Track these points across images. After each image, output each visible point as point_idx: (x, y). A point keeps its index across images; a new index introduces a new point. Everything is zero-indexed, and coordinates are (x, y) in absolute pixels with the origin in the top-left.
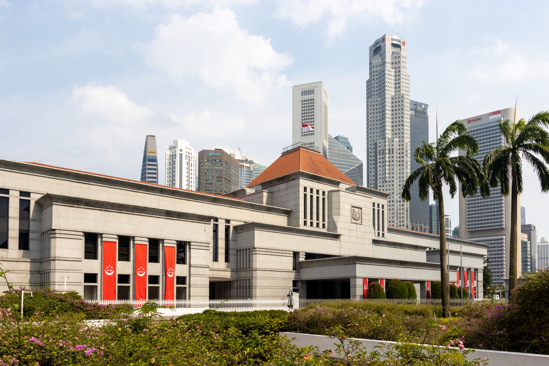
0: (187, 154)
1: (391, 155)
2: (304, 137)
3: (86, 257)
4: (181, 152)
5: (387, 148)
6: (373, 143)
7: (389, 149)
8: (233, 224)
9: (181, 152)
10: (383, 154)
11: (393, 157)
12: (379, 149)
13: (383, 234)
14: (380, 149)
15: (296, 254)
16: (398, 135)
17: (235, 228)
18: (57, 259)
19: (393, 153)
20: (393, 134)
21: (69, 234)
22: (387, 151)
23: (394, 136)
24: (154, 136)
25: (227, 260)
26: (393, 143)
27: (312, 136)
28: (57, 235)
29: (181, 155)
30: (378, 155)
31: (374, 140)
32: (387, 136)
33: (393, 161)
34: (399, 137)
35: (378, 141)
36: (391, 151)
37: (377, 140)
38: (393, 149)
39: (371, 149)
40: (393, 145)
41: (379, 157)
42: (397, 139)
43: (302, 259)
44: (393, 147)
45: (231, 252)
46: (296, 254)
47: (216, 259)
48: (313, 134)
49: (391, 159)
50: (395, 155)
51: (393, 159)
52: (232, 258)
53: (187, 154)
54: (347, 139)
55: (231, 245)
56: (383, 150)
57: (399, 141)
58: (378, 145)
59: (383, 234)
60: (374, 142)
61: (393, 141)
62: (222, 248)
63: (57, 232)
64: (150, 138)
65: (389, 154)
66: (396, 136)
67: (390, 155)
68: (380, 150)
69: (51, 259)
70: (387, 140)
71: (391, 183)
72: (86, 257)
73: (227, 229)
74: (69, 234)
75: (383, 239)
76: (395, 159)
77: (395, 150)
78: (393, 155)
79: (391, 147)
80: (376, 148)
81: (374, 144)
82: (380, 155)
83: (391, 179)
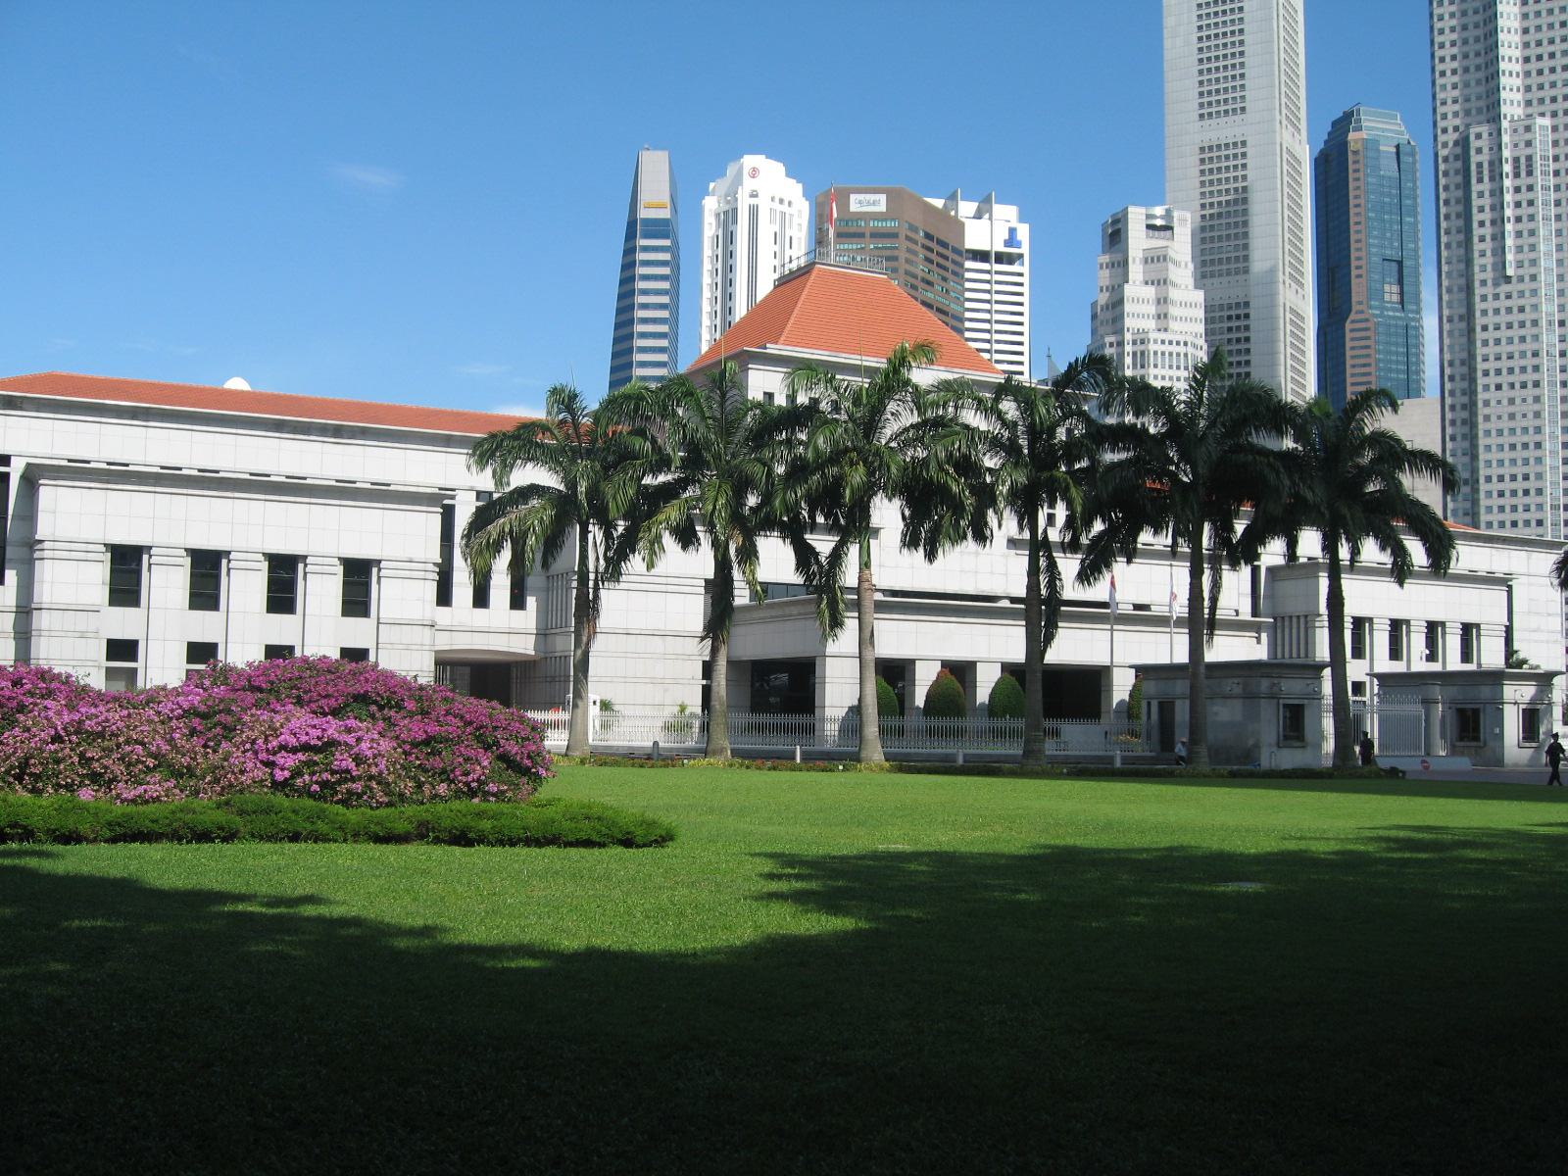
1: (1523, 181)
2: (1206, 122)
3: (113, 602)
4: (754, 201)
5: (1506, 153)
7: (1516, 160)
9: (754, 201)
10: (1492, 179)
11: (1530, 188)
12: (1474, 159)
16: (1548, 107)
18: (44, 606)
19: (1530, 173)
20: (1529, 103)
21: (77, 552)
22: (1507, 168)
23: (1535, 109)
25: (517, 602)
26: (1528, 136)
27: (1238, 118)
28: (47, 554)
29: (754, 212)
30: (1474, 180)
31: (1456, 129)
32: (1504, 109)
33: (1531, 203)
34: (1554, 114)
35: (1473, 131)
36: (1525, 166)
37: (1468, 126)
38: (1529, 158)
39: (1446, 159)
40: (1529, 144)
41: (1475, 187)
42: (1547, 122)
44: (1529, 151)
48: (1243, 109)
49: (1524, 196)
50: (1539, 180)
51: (1530, 195)
53: (776, 205)
56: (1491, 163)
57: (1555, 129)
58: (1474, 144)
61: (1528, 129)
63: (46, 545)
65: (1517, 175)
66: (1542, 109)
67: (1518, 182)
68: (1480, 165)
69: (33, 606)
70: (1505, 124)
71: (1527, 286)
72: (113, 602)
74: (77, 552)
76: (1539, 195)
77: (1538, 163)
78: (1530, 180)
79: (1523, 152)
80: (1465, 157)
83: (1527, 271)
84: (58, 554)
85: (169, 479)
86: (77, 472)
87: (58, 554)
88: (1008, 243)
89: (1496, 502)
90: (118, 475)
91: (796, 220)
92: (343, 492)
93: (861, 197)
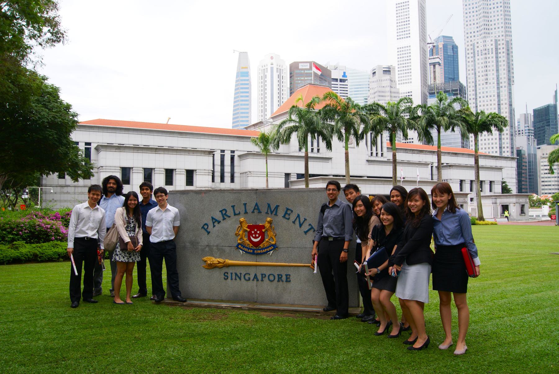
0: (278, 67)
2: (399, 40)
6: (470, 43)
8: (236, 154)
12: (476, 49)
13: (382, 154)
14: (478, 49)
15: (287, 175)
17: (240, 156)
24: (246, 53)
29: (272, 68)
30: (476, 55)
41: (477, 57)
43: (293, 178)
45: (236, 175)
46: (287, 175)
47: (222, 180)
52: (236, 179)
54: (451, 37)
55: (236, 169)
58: (476, 45)
59: (382, 154)
60: (472, 43)
62: (228, 172)
64: (243, 56)
68: (478, 51)
73: (232, 158)
75: (379, 158)
81: (471, 45)
82: (478, 55)
84: (107, 170)
85: (136, 148)
86: (109, 147)
87: (107, 170)
88: (343, 76)
89: (494, 146)
90: (120, 148)
91: (284, 71)
92: (184, 151)
93: (302, 64)
